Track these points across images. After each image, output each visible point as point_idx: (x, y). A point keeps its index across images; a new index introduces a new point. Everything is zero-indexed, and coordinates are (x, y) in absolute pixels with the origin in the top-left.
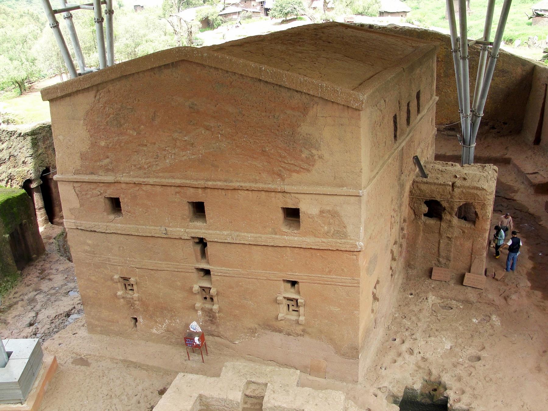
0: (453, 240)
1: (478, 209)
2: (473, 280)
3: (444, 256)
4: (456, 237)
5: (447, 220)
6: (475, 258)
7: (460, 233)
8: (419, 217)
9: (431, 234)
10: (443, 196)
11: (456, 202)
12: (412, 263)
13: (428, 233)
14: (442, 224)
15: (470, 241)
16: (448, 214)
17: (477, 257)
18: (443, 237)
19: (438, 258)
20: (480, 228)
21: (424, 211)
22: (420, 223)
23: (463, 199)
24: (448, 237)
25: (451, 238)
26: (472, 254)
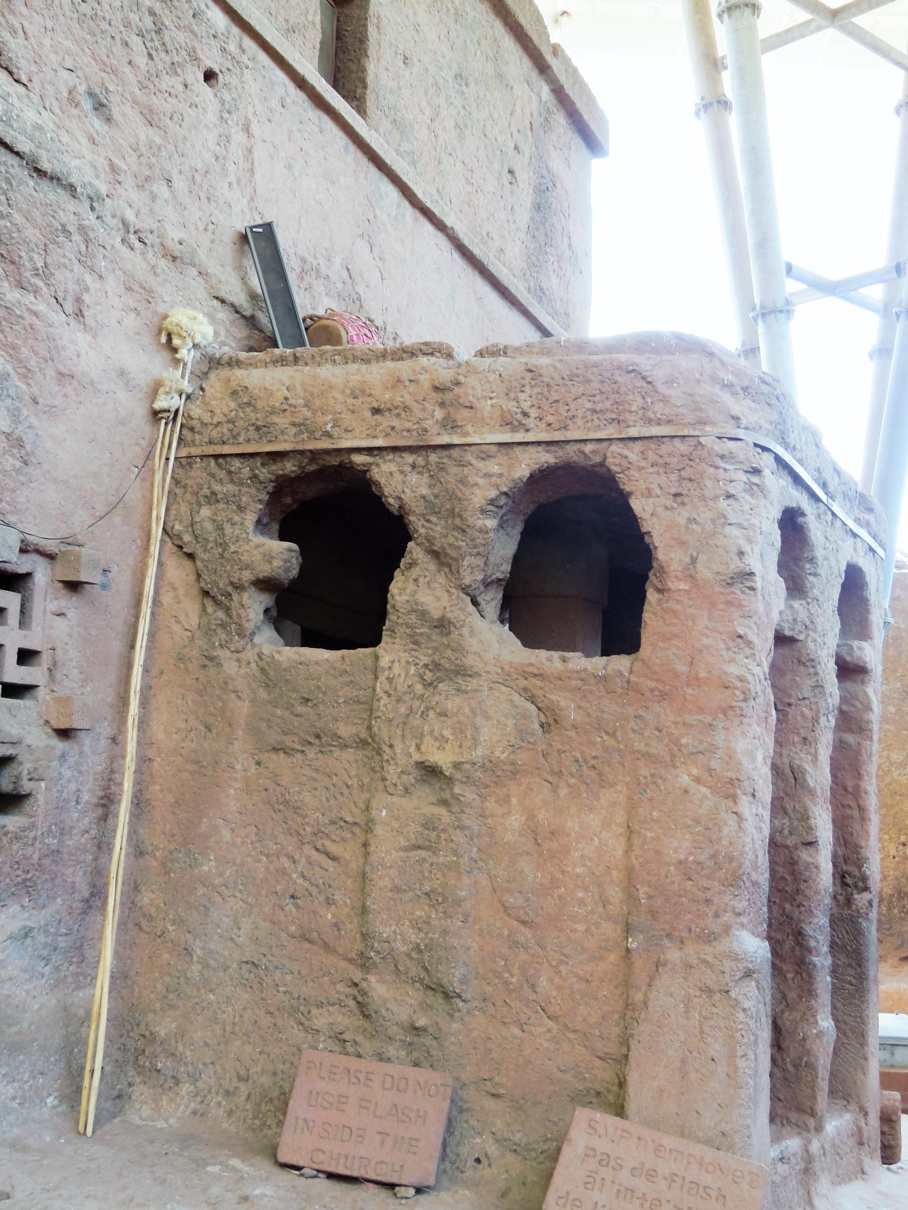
0: (468, 794)
1: (648, 494)
2: (641, 1185)
3: (402, 948)
4: (490, 766)
5: (423, 615)
6: (658, 965)
7: (521, 733)
8: (227, 610)
9: (311, 754)
10: (386, 421)
11: (484, 452)
12: (164, 1027)
13: (286, 751)
14: (384, 662)
15: (606, 797)
16: (432, 567)
17: (674, 955)
18: (392, 772)
19: (357, 976)
20: (682, 668)
21: (257, 557)
22: (230, 667)
23: (530, 422)
24: (430, 772)
25: (450, 780)
26: (628, 930)
